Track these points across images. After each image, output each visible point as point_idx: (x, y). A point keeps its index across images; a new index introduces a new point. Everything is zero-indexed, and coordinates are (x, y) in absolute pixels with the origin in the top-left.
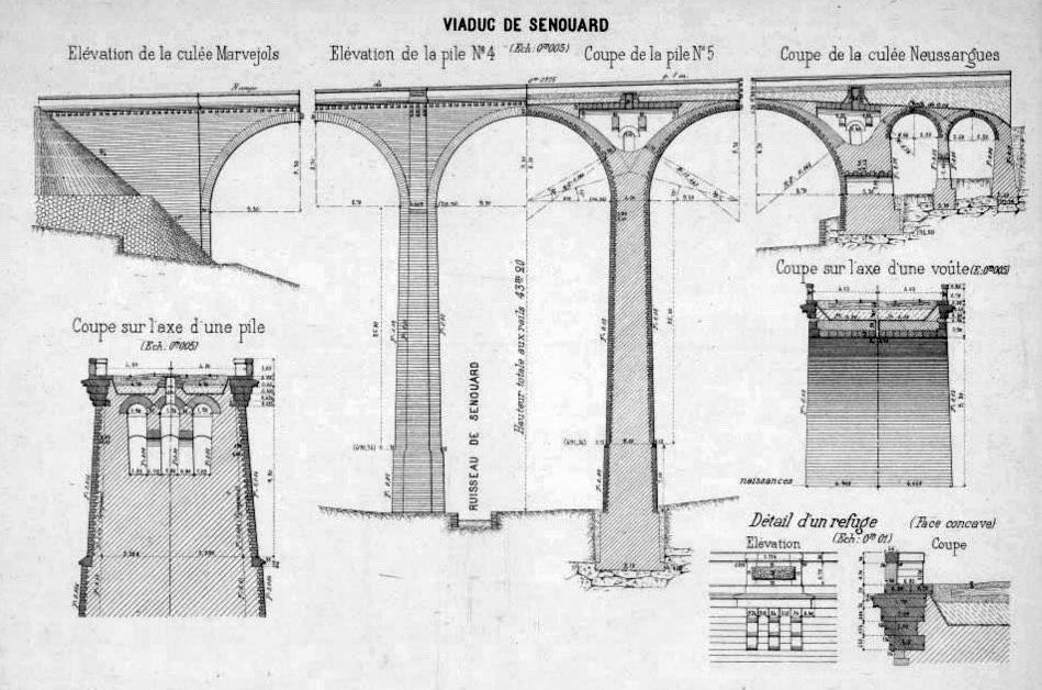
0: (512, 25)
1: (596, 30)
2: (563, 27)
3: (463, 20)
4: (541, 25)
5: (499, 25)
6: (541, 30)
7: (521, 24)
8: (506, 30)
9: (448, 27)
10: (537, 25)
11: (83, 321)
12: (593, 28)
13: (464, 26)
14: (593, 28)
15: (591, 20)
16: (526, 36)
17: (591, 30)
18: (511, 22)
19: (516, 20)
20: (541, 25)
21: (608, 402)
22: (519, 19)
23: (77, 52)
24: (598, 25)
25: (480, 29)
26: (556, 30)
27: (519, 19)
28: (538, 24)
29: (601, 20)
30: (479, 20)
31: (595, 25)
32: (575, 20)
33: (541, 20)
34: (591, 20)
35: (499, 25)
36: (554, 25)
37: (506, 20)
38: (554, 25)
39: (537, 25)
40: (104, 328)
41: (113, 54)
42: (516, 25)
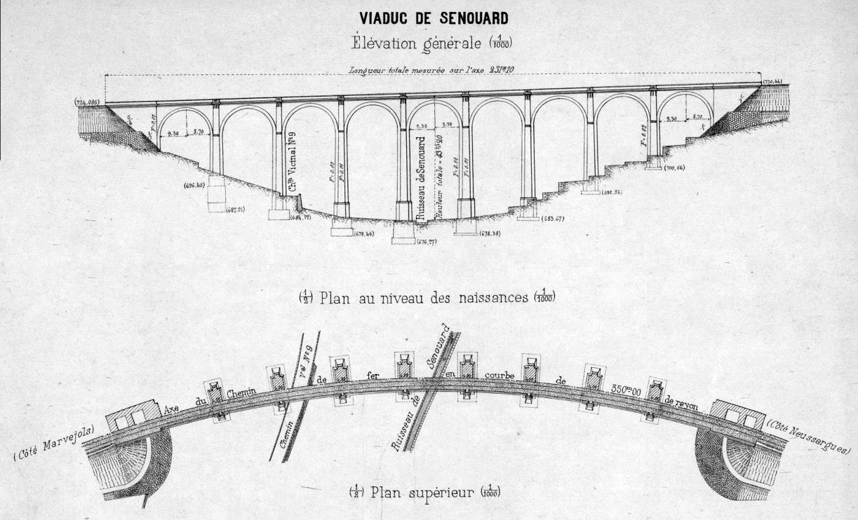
0: (423, 18)
1: (498, 23)
2: (471, 20)
3: (377, 14)
4: (451, 18)
5: (411, 18)
6: (451, 23)
7: (431, 18)
8: (418, 23)
9: (364, 21)
10: (447, 18)
11: (821, 447)
12: (496, 20)
13: (379, 20)
14: (496, 20)
15: (494, 13)
16: (436, 29)
17: (494, 23)
18: (401, 21)
19: (426, 13)
20: (451, 18)
21: (294, 441)
22: (430, 13)
23: (361, 42)
24: (500, 18)
25: (477, 23)
26: (464, 23)
27: (430, 13)
28: (448, 17)
29: (503, 13)
30: (477, 13)
31: (497, 18)
32: (481, 13)
33: (451, 13)
34: (494, 13)
35: (411, 18)
36: (463, 18)
37: (418, 13)
38: (463, 18)
39: (447, 18)
40: (429, 494)
41: (396, 43)
42: (427, 18)
